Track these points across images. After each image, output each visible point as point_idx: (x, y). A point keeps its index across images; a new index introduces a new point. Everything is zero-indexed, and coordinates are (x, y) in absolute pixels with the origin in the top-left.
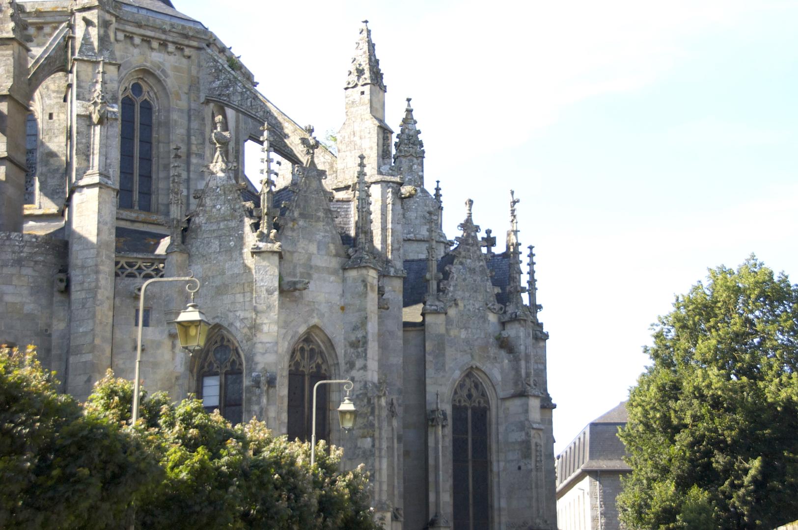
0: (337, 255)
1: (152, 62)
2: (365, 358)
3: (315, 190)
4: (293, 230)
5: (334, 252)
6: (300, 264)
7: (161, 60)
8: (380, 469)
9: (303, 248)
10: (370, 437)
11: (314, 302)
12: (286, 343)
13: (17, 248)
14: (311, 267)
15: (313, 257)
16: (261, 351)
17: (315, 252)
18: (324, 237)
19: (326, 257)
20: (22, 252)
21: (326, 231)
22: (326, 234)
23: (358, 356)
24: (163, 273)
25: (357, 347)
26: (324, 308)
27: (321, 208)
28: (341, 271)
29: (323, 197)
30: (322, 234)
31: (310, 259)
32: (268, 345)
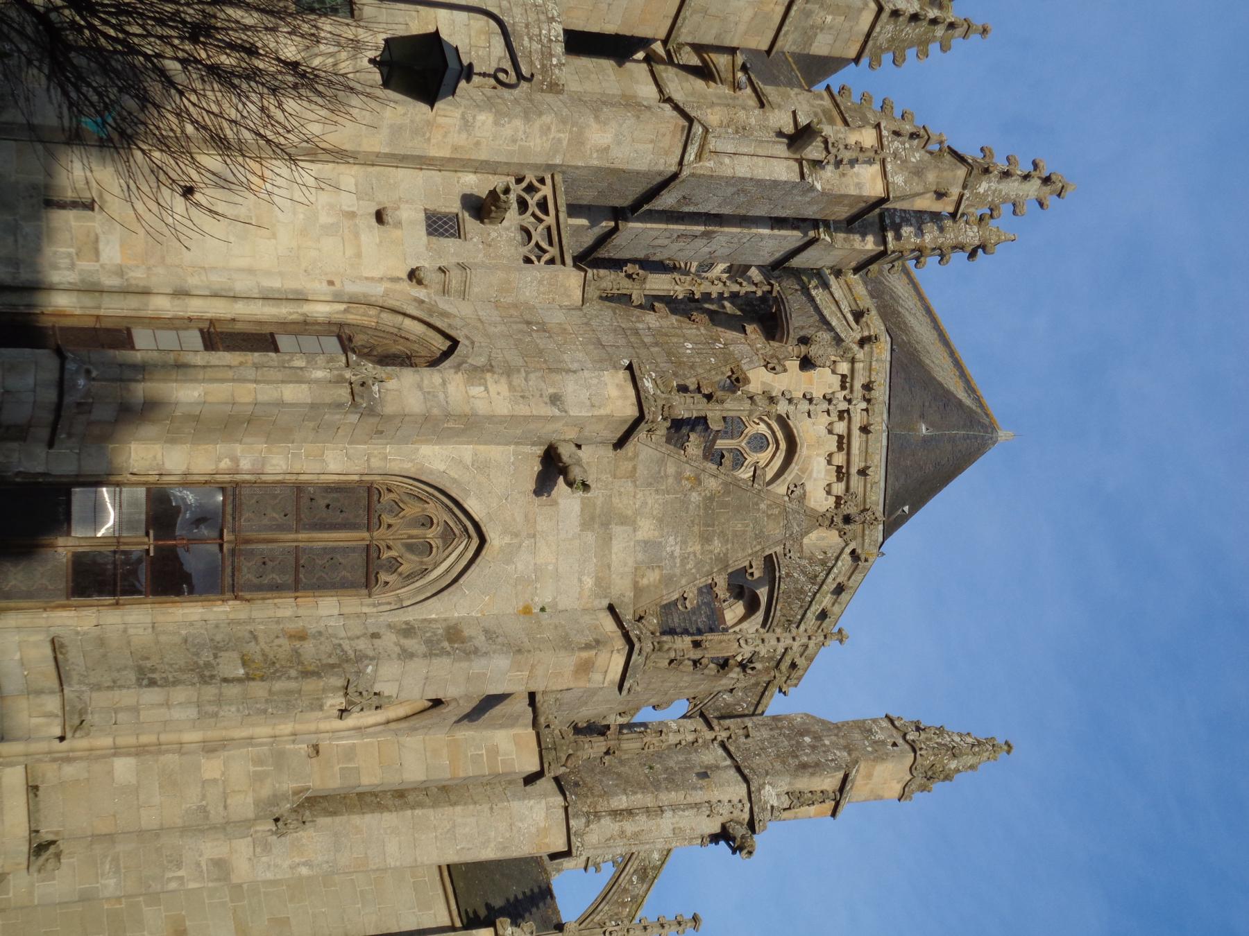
0: (638, 590)
1: (809, 457)
2: (429, 655)
3: (761, 531)
4: (679, 476)
5: (645, 582)
6: (610, 496)
7: (815, 475)
8: (167, 704)
9: (645, 503)
10: (247, 674)
11: (534, 536)
12: (442, 467)
13: (536, 31)
14: (606, 525)
15: (629, 529)
16: (426, 382)
17: (640, 535)
18: (672, 554)
19: (631, 562)
20: (531, 39)
21: (684, 559)
22: (678, 561)
23: (428, 642)
24: (536, 262)
25: (450, 641)
26: (522, 564)
27: (729, 546)
28: (605, 603)
29: (750, 551)
30: (677, 553)
31: (624, 520)
32: (441, 396)
